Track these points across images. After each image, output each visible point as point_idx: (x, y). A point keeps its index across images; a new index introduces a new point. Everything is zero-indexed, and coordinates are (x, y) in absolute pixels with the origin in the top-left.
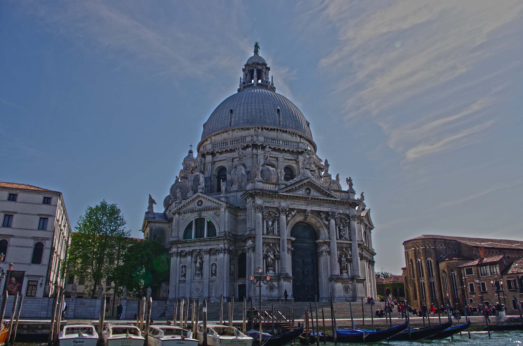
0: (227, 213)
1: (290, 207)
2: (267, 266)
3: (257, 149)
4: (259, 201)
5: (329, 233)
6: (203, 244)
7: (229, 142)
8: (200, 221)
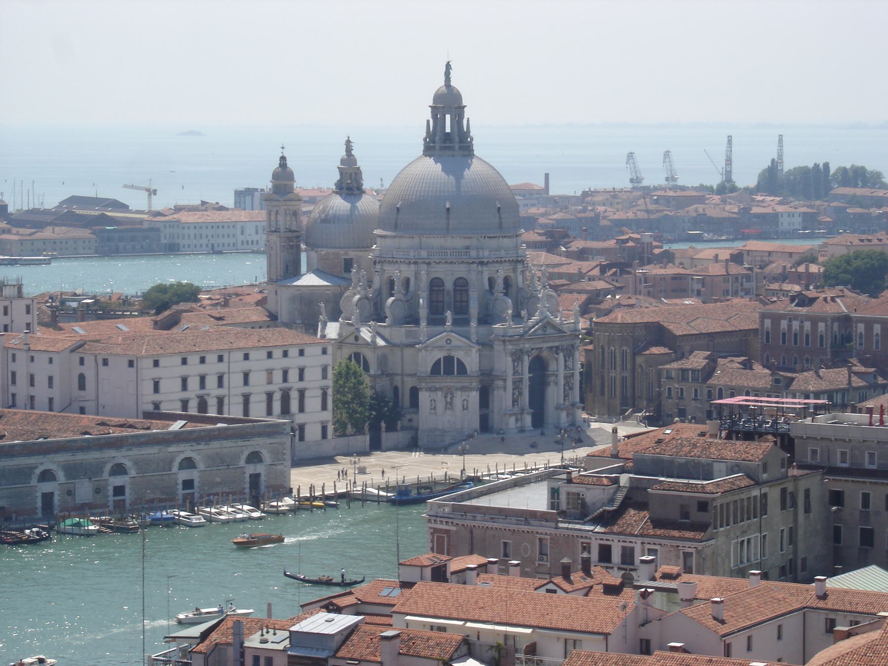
0: (478, 354)
1: (532, 347)
2: (513, 402)
3: (482, 265)
4: (510, 347)
5: (557, 365)
6: (454, 381)
7: (449, 253)
8: (449, 360)
